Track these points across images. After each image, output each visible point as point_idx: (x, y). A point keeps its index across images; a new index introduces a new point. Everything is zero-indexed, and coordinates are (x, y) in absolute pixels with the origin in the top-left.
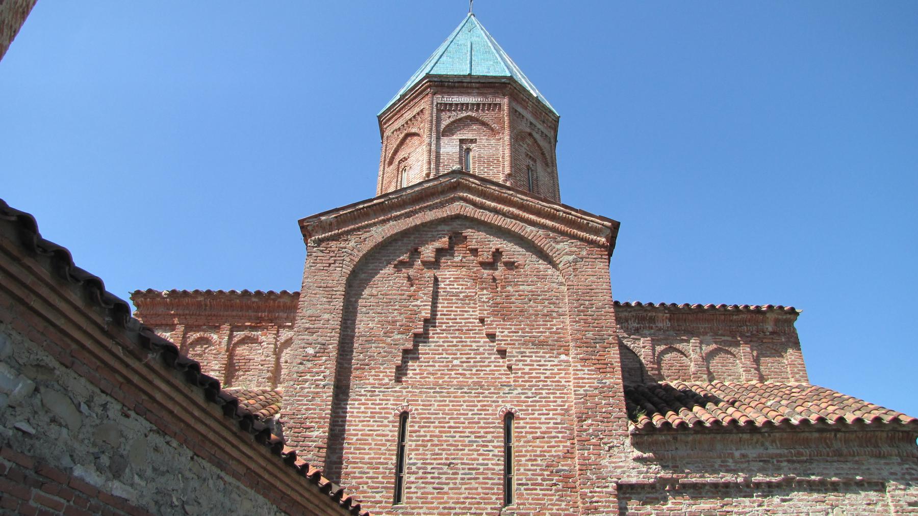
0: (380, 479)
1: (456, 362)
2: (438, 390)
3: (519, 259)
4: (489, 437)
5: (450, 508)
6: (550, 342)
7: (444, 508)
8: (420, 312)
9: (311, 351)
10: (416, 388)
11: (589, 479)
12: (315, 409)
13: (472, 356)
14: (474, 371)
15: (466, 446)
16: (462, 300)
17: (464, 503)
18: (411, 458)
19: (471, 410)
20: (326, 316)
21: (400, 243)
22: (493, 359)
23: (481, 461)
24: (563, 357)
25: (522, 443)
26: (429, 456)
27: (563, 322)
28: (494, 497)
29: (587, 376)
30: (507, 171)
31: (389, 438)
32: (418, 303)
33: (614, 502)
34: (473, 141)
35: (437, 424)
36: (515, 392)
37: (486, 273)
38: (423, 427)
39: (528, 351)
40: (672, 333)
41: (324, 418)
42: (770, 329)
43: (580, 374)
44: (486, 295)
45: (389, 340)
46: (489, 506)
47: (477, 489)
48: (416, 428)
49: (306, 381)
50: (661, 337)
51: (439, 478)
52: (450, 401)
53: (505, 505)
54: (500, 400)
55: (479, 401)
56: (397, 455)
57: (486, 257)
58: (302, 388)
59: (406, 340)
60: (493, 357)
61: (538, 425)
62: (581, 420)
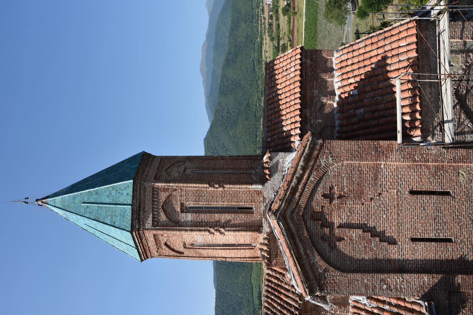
0: (443, 249)
1: (384, 217)
2: (400, 225)
3: (328, 185)
4: (421, 201)
5: (453, 218)
6: (375, 172)
7: (453, 221)
8: (360, 234)
9: (385, 287)
10: (399, 235)
11: (441, 160)
12: (414, 281)
13: (381, 209)
14: (389, 208)
15: (426, 212)
16: (351, 214)
17: (451, 212)
18: (432, 236)
19: (409, 209)
20: (365, 281)
21: (318, 246)
22: (383, 199)
23: (433, 205)
24: (382, 166)
25: (424, 187)
26: (431, 228)
27: (364, 165)
28: (448, 200)
29: (395, 157)
30: (208, 186)
31: (423, 246)
32: (354, 235)
33: (451, 151)
34: (182, 205)
35: (416, 225)
36: (400, 189)
37: (335, 202)
38: (418, 231)
39: (379, 183)
40: (313, 109)
41: (419, 277)
42: (310, 62)
43: (394, 159)
44: (349, 203)
45: (375, 249)
46: (452, 202)
47: (444, 207)
48: (419, 234)
49: (401, 288)
50: (315, 114)
51: (441, 223)
52: (405, 219)
53: (450, 195)
54: (404, 196)
55: (405, 206)
56: (431, 242)
57: (326, 201)
58: (404, 288)
59: (375, 241)
60: (381, 199)
61: (415, 180)
62: (415, 161)
